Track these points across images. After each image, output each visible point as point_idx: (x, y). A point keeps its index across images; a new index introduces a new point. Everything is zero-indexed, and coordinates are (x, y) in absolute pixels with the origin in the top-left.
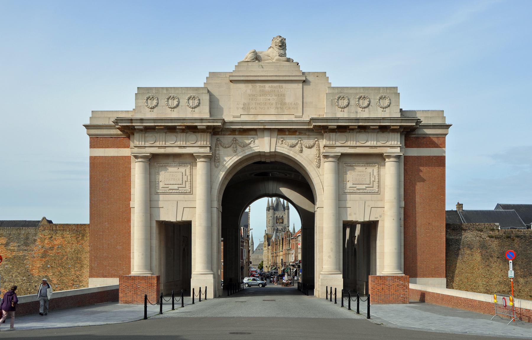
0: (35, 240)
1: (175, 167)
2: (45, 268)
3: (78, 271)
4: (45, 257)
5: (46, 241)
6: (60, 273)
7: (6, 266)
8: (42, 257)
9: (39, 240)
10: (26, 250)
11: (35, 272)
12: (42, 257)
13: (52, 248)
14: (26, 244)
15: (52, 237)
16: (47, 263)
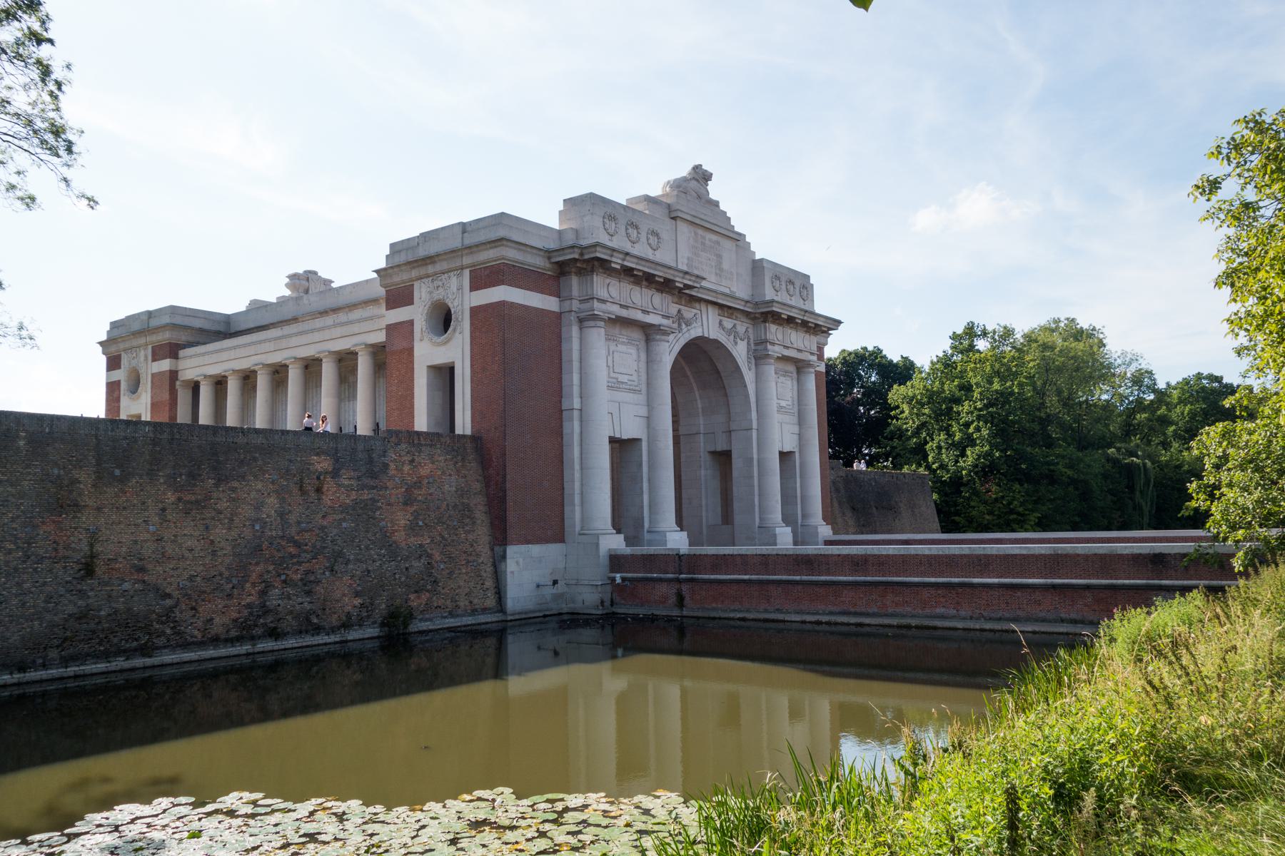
0: (386, 466)
1: (623, 343)
2: (412, 528)
3: (469, 532)
4: (411, 505)
5: (406, 468)
6: (443, 537)
7: (344, 525)
8: (405, 504)
9: (392, 466)
10: (373, 488)
11: (400, 536)
12: (405, 504)
13: (418, 484)
14: (373, 475)
15: (413, 461)
16: (416, 515)
